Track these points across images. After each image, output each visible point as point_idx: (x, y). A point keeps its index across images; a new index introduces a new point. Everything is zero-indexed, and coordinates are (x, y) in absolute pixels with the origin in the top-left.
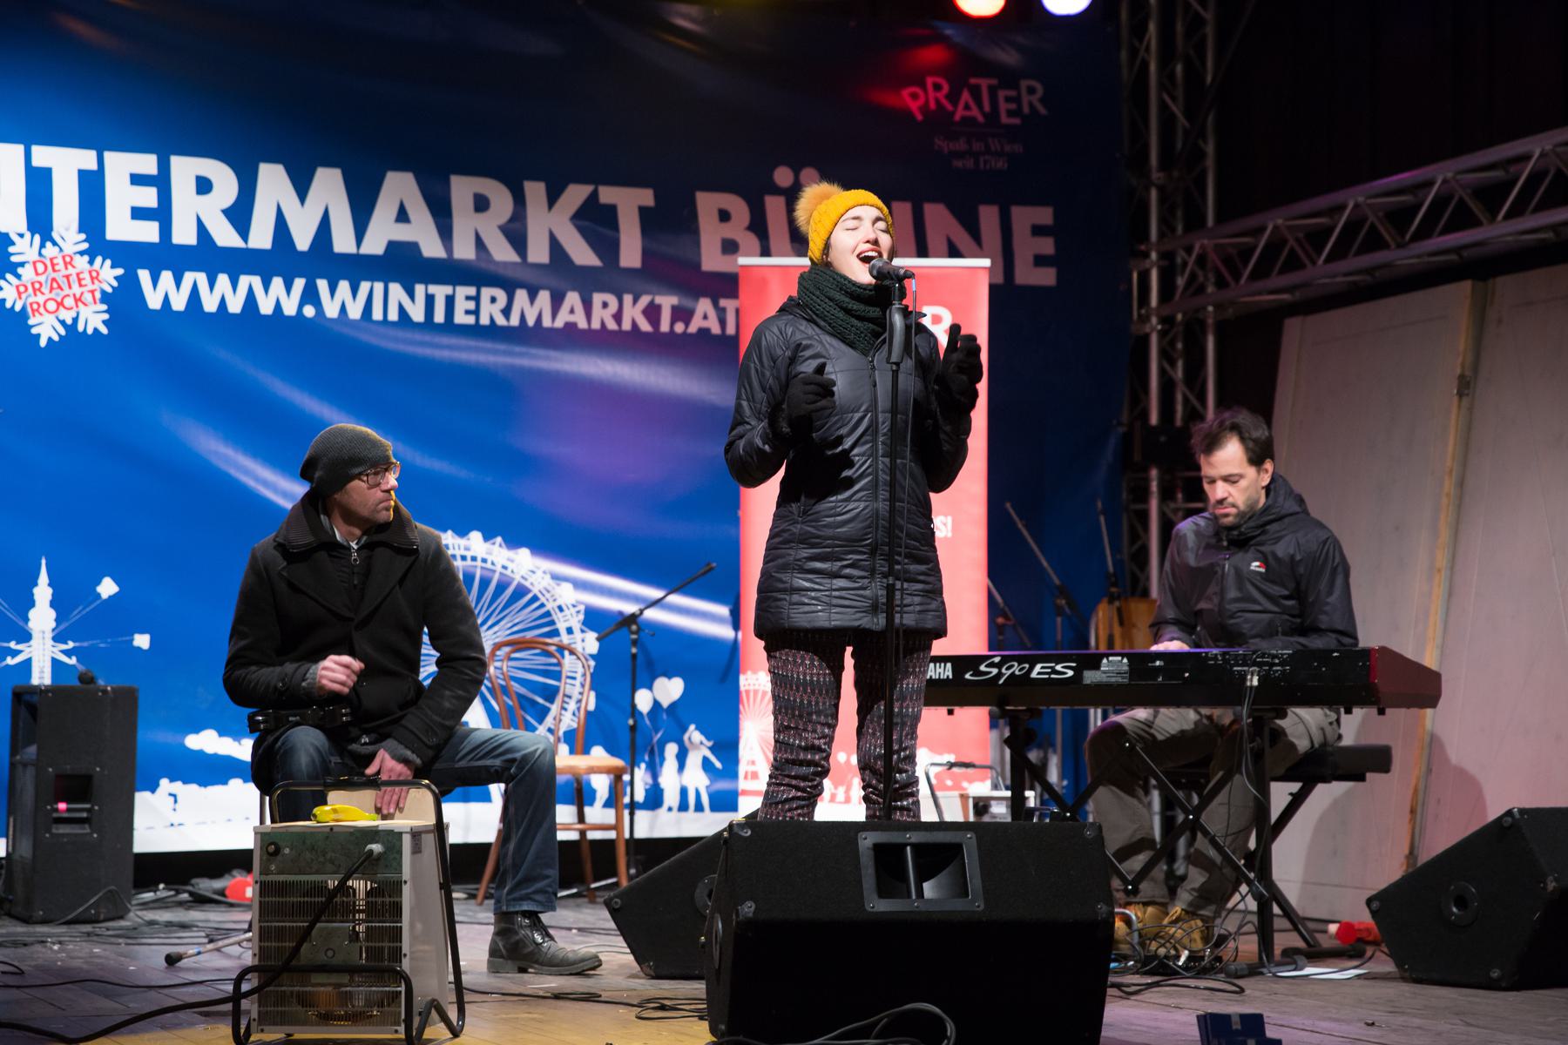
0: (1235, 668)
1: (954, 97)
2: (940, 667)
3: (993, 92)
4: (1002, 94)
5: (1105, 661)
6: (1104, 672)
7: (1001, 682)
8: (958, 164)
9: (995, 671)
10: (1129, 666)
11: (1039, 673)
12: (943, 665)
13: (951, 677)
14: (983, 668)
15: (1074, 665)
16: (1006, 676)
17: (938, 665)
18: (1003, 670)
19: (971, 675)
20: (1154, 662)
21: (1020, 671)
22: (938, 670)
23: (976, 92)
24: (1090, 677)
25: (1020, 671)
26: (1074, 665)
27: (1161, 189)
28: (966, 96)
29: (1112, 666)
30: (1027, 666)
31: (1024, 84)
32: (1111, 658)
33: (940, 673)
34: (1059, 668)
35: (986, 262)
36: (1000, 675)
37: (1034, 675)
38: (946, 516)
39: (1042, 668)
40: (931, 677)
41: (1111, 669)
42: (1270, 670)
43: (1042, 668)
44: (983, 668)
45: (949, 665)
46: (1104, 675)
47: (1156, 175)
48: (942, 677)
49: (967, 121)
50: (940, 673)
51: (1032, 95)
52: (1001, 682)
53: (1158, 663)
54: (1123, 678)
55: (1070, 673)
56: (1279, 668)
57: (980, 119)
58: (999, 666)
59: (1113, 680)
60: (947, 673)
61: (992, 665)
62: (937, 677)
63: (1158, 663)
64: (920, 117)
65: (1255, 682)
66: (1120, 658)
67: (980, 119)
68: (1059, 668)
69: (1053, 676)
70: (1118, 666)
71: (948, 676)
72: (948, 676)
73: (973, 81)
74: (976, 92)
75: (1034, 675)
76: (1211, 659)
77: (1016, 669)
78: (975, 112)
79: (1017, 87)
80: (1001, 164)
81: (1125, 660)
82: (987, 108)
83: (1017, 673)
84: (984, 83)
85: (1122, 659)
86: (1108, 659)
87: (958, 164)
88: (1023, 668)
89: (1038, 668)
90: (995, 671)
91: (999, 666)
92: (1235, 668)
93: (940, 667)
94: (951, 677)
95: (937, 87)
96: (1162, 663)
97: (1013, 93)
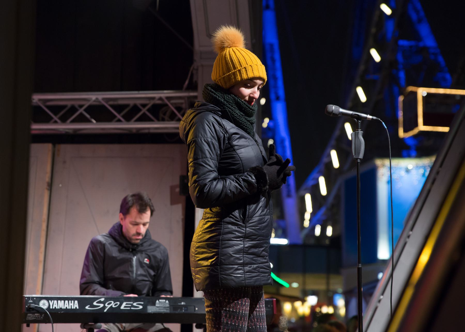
2: (71, 303)
5: (157, 302)
6: (158, 307)
7: (105, 311)
9: (102, 305)
10: (169, 304)
11: (125, 307)
12: (73, 301)
13: (78, 308)
14: (95, 304)
15: (142, 303)
17: (70, 301)
18: (106, 305)
19: (89, 307)
21: (115, 305)
22: (70, 304)
24: (151, 309)
25: (115, 305)
26: (142, 303)
29: (161, 304)
30: (118, 303)
32: (160, 300)
33: (71, 306)
34: (135, 304)
36: (104, 307)
37: (122, 307)
39: (127, 304)
40: (55, 307)
41: (160, 305)
43: (127, 304)
44: (95, 304)
45: (76, 302)
46: (157, 308)
48: (73, 308)
50: (71, 306)
52: (105, 311)
54: (167, 310)
55: (141, 307)
58: (104, 303)
60: (75, 306)
61: (100, 302)
62: (70, 308)
66: (164, 301)
68: (135, 304)
69: (132, 308)
70: (164, 304)
71: (76, 307)
72: (76, 307)
75: (122, 307)
77: (113, 304)
81: (167, 302)
83: (114, 306)
85: (166, 301)
86: (159, 301)
88: (117, 304)
89: (124, 304)
90: (102, 305)
91: (104, 303)
93: (71, 303)
94: (78, 308)
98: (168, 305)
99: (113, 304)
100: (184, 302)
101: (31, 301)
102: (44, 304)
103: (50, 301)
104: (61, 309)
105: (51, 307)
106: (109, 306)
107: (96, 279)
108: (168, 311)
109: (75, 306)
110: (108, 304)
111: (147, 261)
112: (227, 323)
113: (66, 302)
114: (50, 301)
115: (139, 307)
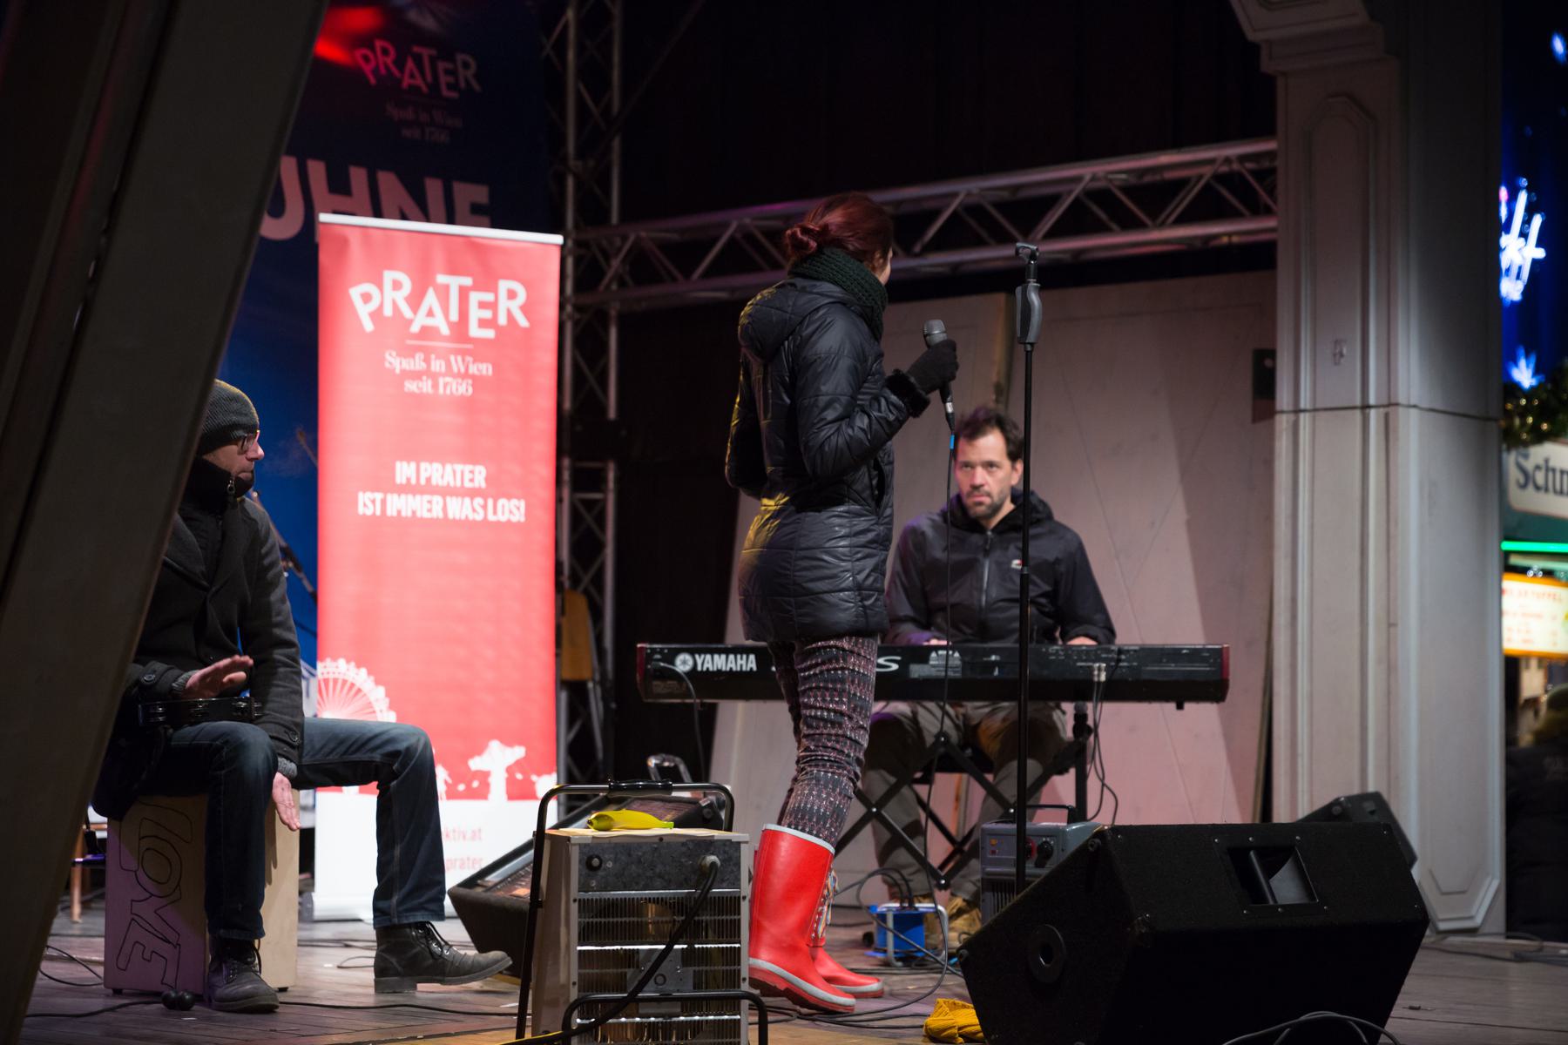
0: (1079, 664)
1: (400, 64)
3: (433, 60)
4: (441, 66)
5: (933, 655)
6: (933, 666)
8: (406, 133)
12: (745, 656)
13: (755, 669)
15: (898, 658)
17: (739, 656)
20: (989, 656)
22: (739, 662)
23: (418, 60)
24: (917, 671)
26: (898, 658)
27: (577, 177)
28: (410, 65)
31: (460, 57)
35: (558, 239)
38: (518, 498)
42: (1117, 666)
45: (752, 657)
46: (933, 669)
47: (572, 162)
48: (744, 669)
49: (415, 90)
51: (467, 68)
53: (993, 658)
54: (955, 672)
55: (895, 667)
57: (424, 89)
62: (739, 669)
64: (373, 81)
65: (1103, 678)
67: (424, 89)
73: (416, 49)
74: (418, 60)
76: (1052, 654)
78: (419, 82)
79: (450, 57)
80: (443, 138)
82: (429, 79)
84: (426, 53)
87: (406, 133)
94: (755, 669)
95: (385, 52)
97: (450, 66)
101: (658, 656)
102: (684, 662)
103: (697, 656)
104: (719, 672)
105: (699, 668)
107: (905, 609)
109: (750, 665)
111: (1018, 565)
112: (855, 694)
113: (732, 657)
114: (697, 656)
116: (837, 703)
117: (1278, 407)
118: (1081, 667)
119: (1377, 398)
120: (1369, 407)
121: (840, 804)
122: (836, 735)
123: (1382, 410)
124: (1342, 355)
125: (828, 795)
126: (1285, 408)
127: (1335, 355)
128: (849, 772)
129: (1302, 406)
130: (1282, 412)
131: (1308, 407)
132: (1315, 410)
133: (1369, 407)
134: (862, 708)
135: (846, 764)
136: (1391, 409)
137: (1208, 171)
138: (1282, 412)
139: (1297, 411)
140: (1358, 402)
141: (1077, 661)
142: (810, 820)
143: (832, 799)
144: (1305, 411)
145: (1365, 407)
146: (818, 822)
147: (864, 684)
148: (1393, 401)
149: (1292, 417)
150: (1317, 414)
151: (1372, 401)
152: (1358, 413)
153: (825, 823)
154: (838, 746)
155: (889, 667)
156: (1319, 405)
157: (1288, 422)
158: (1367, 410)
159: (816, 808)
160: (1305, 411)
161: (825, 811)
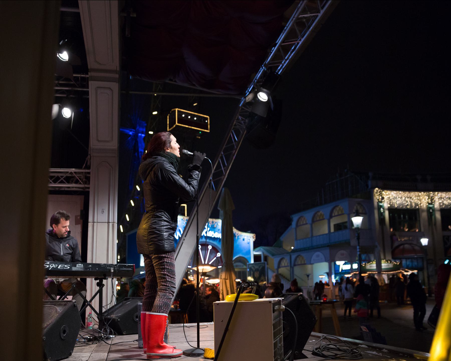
0: (107, 268)
5: (77, 265)
6: (77, 268)
7: (50, 269)
9: (48, 266)
11: (60, 267)
16: (51, 268)
18: (50, 266)
20: (89, 266)
21: (55, 266)
24: (74, 269)
25: (55, 266)
29: (79, 266)
30: (57, 265)
32: (79, 264)
34: (65, 266)
36: (49, 267)
37: (59, 268)
39: (61, 266)
43: (61, 266)
52: (50, 269)
53: (90, 266)
54: (82, 269)
55: (69, 268)
56: (116, 268)
58: (49, 265)
59: (80, 270)
63: (90, 266)
65: (113, 271)
68: (65, 266)
69: (64, 268)
75: (59, 268)
77: (54, 266)
81: (82, 265)
83: (54, 267)
88: (56, 266)
89: (60, 266)
90: (48, 266)
92: (107, 268)
96: (91, 266)
98: (83, 267)
99: (54, 266)
100: (91, 265)
106: (52, 267)
108: (83, 270)
110: (51, 266)
115: (68, 268)
116: (163, 271)
117: (89, 221)
118: (108, 269)
119: (111, 221)
120: (110, 222)
121: (166, 301)
122: (165, 281)
123: (112, 223)
124: (104, 212)
125: (162, 300)
126: (91, 222)
127: (102, 212)
128: (169, 291)
129: (95, 221)
130: (90, 222)
131: (96, 221)
132: (97, 222)
133: (110, 222)
134: (171, 272)
135: (167, 289)
136: (114, 223)
137: (65, 176)
138: (90, 222)
139: (94, 222)
140: (107, 222)
141: (107, 267)
142: (157, 308)
143: (163, 301)
144: (95, 222)
145: (108, 222)
146: (159, 308)
147: (173, 266)
148: (114, 222)
149: (92, 223)
150: (98, 223)
151: (110, 222)
152: (107, 224)
153: (161, 308)
154: (165, 284)
155: (68, 268)
156: (98, 222)
157: (91, 224)
158: (109, 223)
159: (159, 304)
160: (95, 222)
161: (161, 305)
